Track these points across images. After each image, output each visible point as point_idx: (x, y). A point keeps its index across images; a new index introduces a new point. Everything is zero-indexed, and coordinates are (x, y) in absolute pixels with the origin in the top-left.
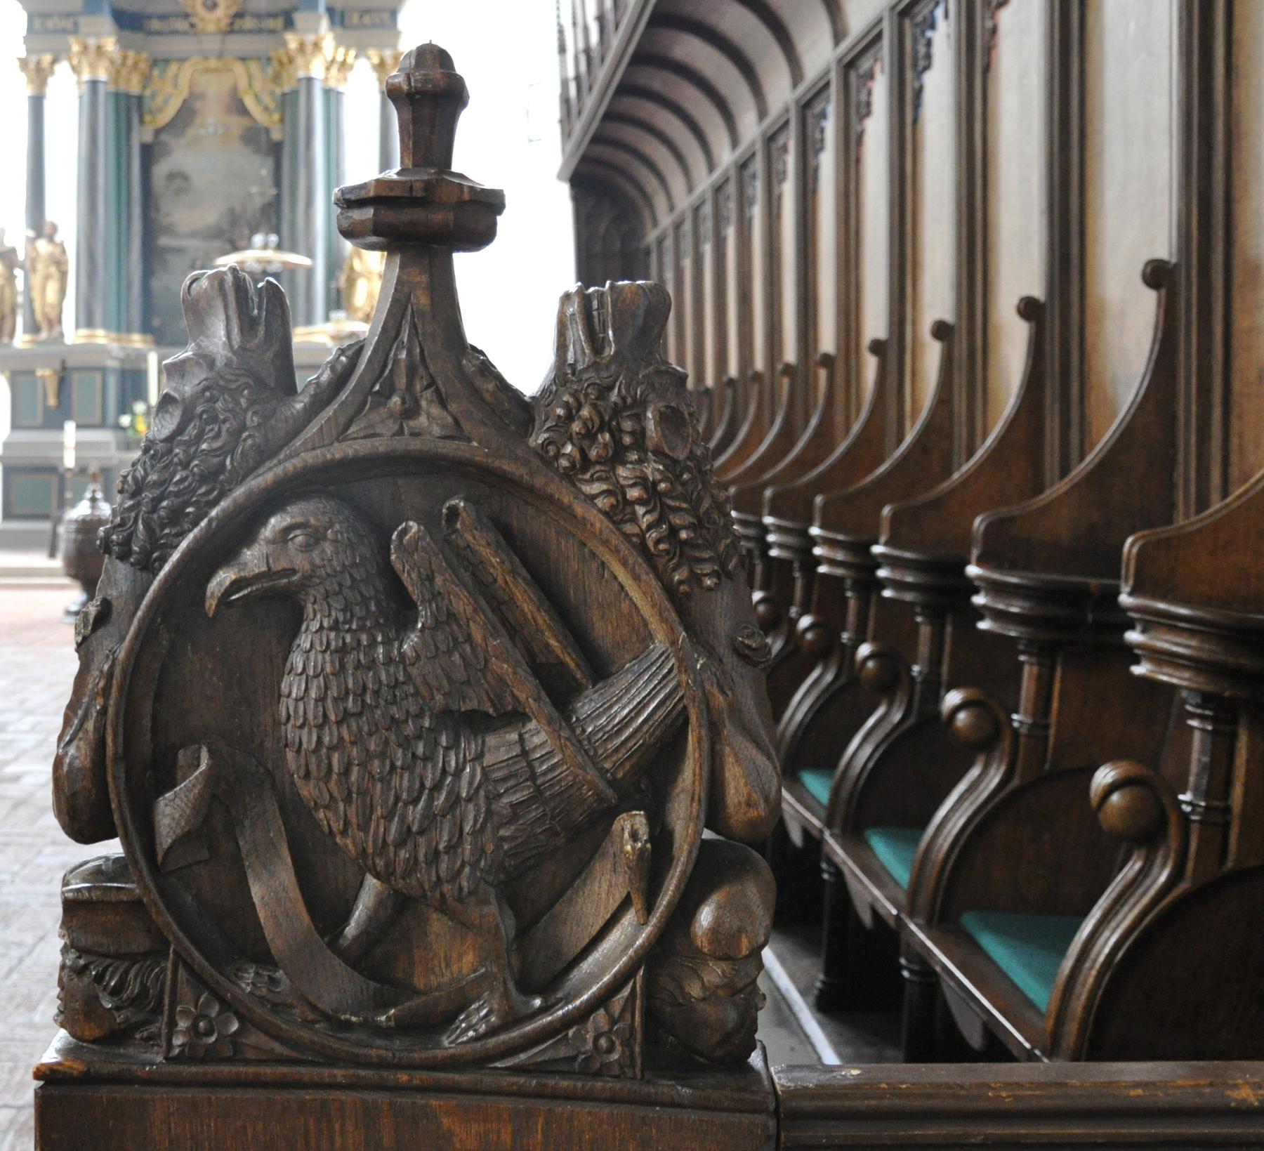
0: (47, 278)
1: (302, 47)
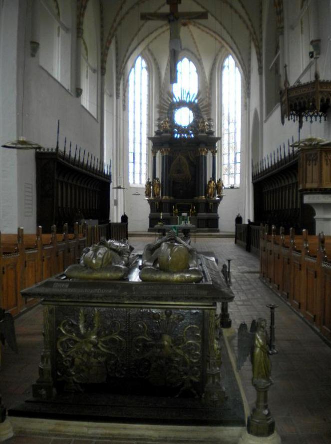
1: (201, 150)
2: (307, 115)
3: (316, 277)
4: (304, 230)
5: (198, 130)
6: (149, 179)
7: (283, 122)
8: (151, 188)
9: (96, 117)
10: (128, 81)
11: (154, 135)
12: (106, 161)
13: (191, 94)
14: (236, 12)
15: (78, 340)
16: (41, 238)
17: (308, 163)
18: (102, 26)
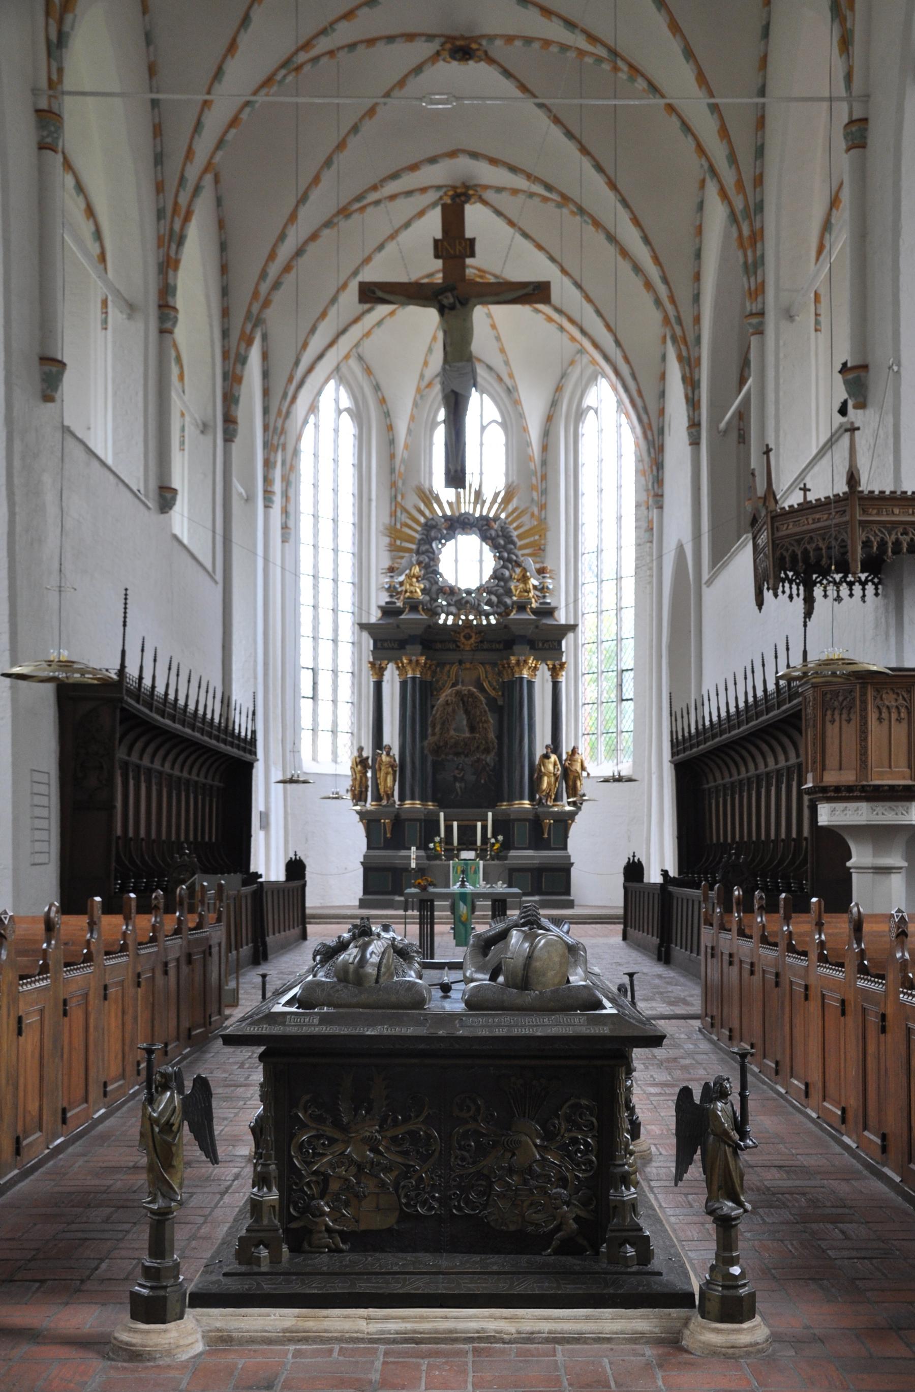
0: (387, 774)
2: (825, 582)
3: (843, 1013)
4: (814, 900)
5: (508, 601)
6: (361, 749)
7: (760, 603)
8: (369, 774)
9: (209, 567)
10: (296, 452)
11: (374, 616)
12: (240, 696)
13: (488, 495)
14: (624, 253)
15: (336, 1136)
16: (134, 927)
17: (828, 717)
18: (225, 292)
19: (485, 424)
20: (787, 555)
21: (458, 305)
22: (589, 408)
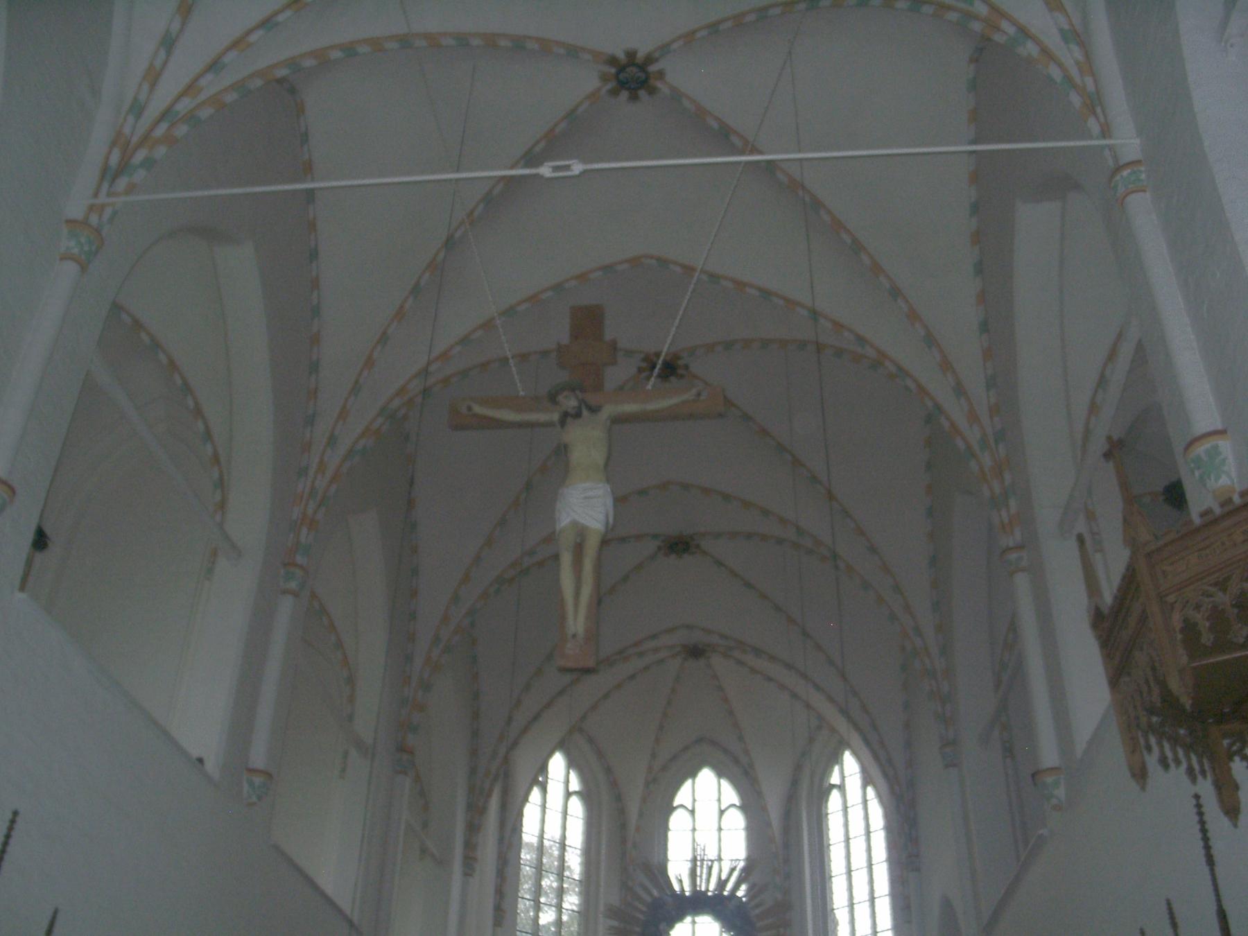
19: (723, 808)
20: (1201, 620)
21: (585, 413)
22: (834, 786)
